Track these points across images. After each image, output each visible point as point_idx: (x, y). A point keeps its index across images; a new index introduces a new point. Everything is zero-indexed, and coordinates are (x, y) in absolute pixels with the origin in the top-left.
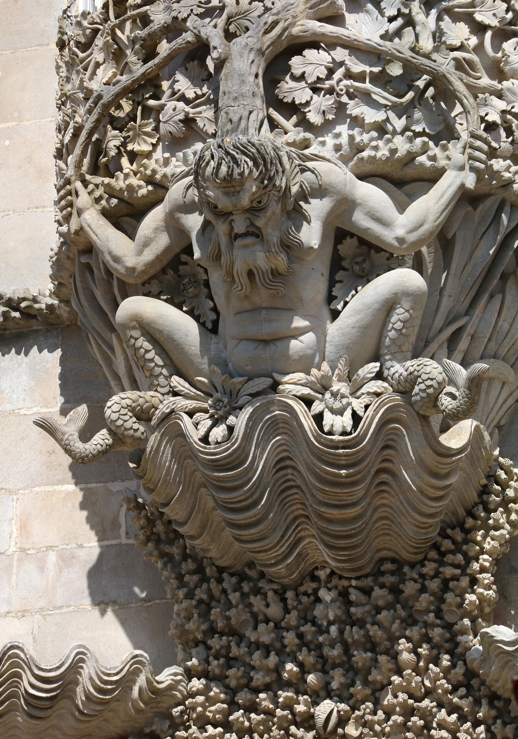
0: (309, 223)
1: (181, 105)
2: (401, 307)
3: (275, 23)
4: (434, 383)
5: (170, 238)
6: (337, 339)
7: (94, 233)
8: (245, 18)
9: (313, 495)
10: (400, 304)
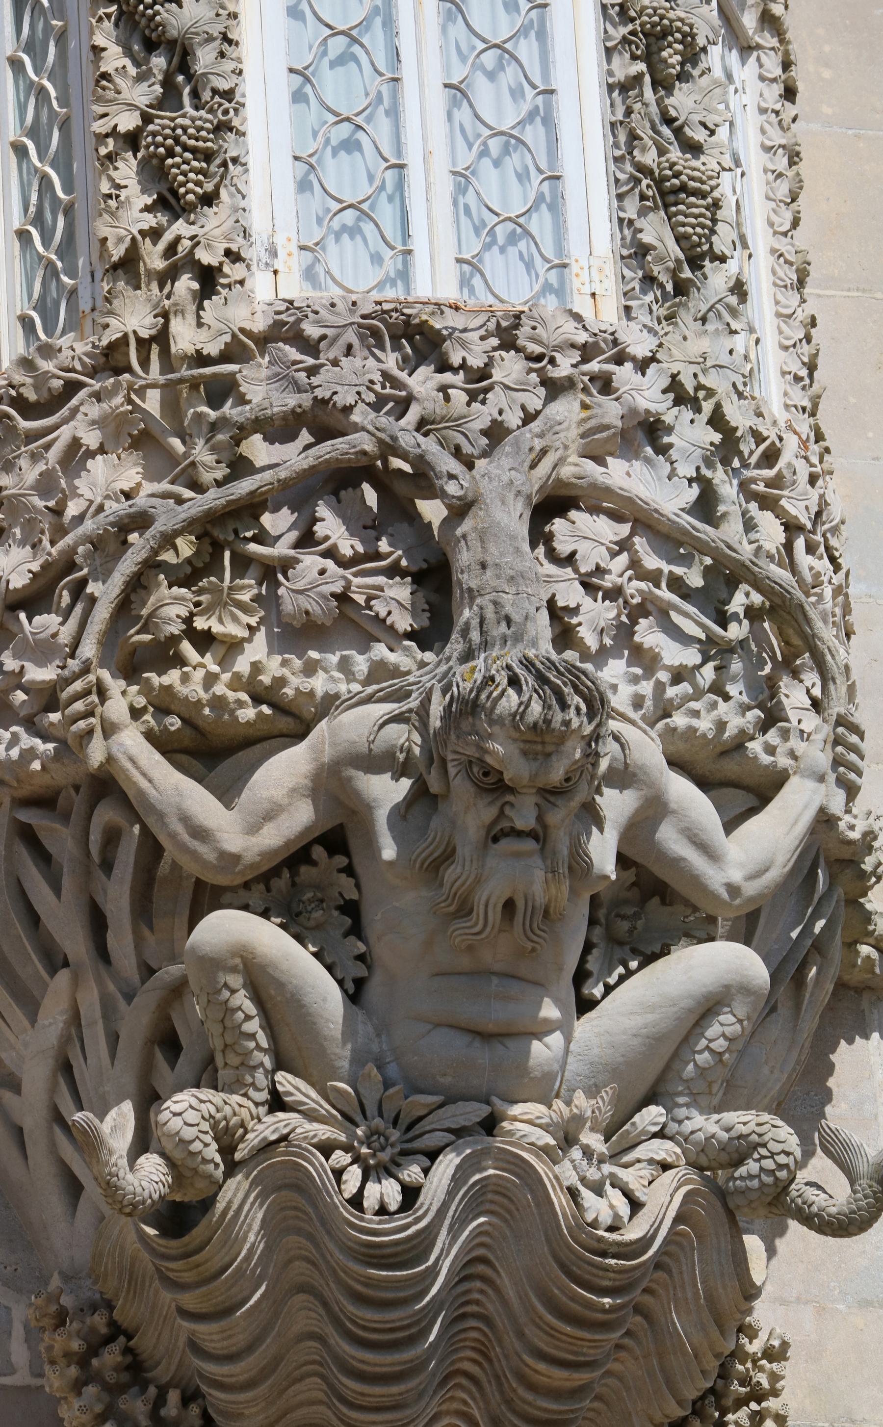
0: (601, 831)
1: (330, 564)
2: (731, 1012)
3: (544, 452)
4: (790, 1160)
5: (316, 811)
6: (596, 1051)
7: (144, 775)
8: (457, 428)
9: (520, 1335)
10: (729, 1006)
